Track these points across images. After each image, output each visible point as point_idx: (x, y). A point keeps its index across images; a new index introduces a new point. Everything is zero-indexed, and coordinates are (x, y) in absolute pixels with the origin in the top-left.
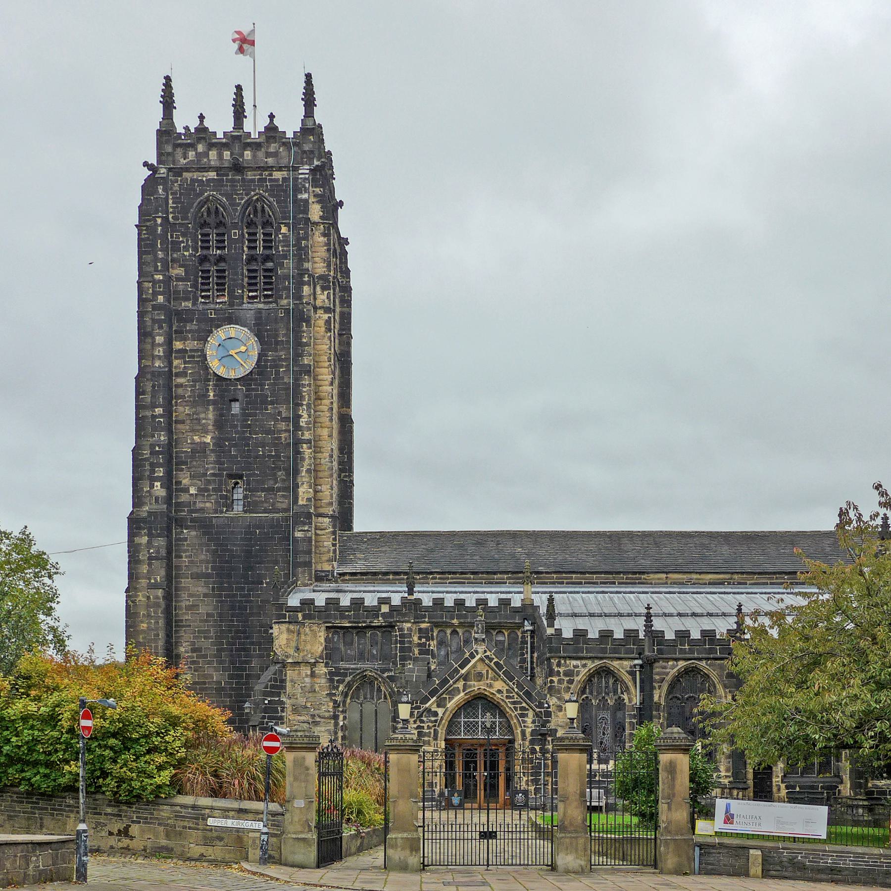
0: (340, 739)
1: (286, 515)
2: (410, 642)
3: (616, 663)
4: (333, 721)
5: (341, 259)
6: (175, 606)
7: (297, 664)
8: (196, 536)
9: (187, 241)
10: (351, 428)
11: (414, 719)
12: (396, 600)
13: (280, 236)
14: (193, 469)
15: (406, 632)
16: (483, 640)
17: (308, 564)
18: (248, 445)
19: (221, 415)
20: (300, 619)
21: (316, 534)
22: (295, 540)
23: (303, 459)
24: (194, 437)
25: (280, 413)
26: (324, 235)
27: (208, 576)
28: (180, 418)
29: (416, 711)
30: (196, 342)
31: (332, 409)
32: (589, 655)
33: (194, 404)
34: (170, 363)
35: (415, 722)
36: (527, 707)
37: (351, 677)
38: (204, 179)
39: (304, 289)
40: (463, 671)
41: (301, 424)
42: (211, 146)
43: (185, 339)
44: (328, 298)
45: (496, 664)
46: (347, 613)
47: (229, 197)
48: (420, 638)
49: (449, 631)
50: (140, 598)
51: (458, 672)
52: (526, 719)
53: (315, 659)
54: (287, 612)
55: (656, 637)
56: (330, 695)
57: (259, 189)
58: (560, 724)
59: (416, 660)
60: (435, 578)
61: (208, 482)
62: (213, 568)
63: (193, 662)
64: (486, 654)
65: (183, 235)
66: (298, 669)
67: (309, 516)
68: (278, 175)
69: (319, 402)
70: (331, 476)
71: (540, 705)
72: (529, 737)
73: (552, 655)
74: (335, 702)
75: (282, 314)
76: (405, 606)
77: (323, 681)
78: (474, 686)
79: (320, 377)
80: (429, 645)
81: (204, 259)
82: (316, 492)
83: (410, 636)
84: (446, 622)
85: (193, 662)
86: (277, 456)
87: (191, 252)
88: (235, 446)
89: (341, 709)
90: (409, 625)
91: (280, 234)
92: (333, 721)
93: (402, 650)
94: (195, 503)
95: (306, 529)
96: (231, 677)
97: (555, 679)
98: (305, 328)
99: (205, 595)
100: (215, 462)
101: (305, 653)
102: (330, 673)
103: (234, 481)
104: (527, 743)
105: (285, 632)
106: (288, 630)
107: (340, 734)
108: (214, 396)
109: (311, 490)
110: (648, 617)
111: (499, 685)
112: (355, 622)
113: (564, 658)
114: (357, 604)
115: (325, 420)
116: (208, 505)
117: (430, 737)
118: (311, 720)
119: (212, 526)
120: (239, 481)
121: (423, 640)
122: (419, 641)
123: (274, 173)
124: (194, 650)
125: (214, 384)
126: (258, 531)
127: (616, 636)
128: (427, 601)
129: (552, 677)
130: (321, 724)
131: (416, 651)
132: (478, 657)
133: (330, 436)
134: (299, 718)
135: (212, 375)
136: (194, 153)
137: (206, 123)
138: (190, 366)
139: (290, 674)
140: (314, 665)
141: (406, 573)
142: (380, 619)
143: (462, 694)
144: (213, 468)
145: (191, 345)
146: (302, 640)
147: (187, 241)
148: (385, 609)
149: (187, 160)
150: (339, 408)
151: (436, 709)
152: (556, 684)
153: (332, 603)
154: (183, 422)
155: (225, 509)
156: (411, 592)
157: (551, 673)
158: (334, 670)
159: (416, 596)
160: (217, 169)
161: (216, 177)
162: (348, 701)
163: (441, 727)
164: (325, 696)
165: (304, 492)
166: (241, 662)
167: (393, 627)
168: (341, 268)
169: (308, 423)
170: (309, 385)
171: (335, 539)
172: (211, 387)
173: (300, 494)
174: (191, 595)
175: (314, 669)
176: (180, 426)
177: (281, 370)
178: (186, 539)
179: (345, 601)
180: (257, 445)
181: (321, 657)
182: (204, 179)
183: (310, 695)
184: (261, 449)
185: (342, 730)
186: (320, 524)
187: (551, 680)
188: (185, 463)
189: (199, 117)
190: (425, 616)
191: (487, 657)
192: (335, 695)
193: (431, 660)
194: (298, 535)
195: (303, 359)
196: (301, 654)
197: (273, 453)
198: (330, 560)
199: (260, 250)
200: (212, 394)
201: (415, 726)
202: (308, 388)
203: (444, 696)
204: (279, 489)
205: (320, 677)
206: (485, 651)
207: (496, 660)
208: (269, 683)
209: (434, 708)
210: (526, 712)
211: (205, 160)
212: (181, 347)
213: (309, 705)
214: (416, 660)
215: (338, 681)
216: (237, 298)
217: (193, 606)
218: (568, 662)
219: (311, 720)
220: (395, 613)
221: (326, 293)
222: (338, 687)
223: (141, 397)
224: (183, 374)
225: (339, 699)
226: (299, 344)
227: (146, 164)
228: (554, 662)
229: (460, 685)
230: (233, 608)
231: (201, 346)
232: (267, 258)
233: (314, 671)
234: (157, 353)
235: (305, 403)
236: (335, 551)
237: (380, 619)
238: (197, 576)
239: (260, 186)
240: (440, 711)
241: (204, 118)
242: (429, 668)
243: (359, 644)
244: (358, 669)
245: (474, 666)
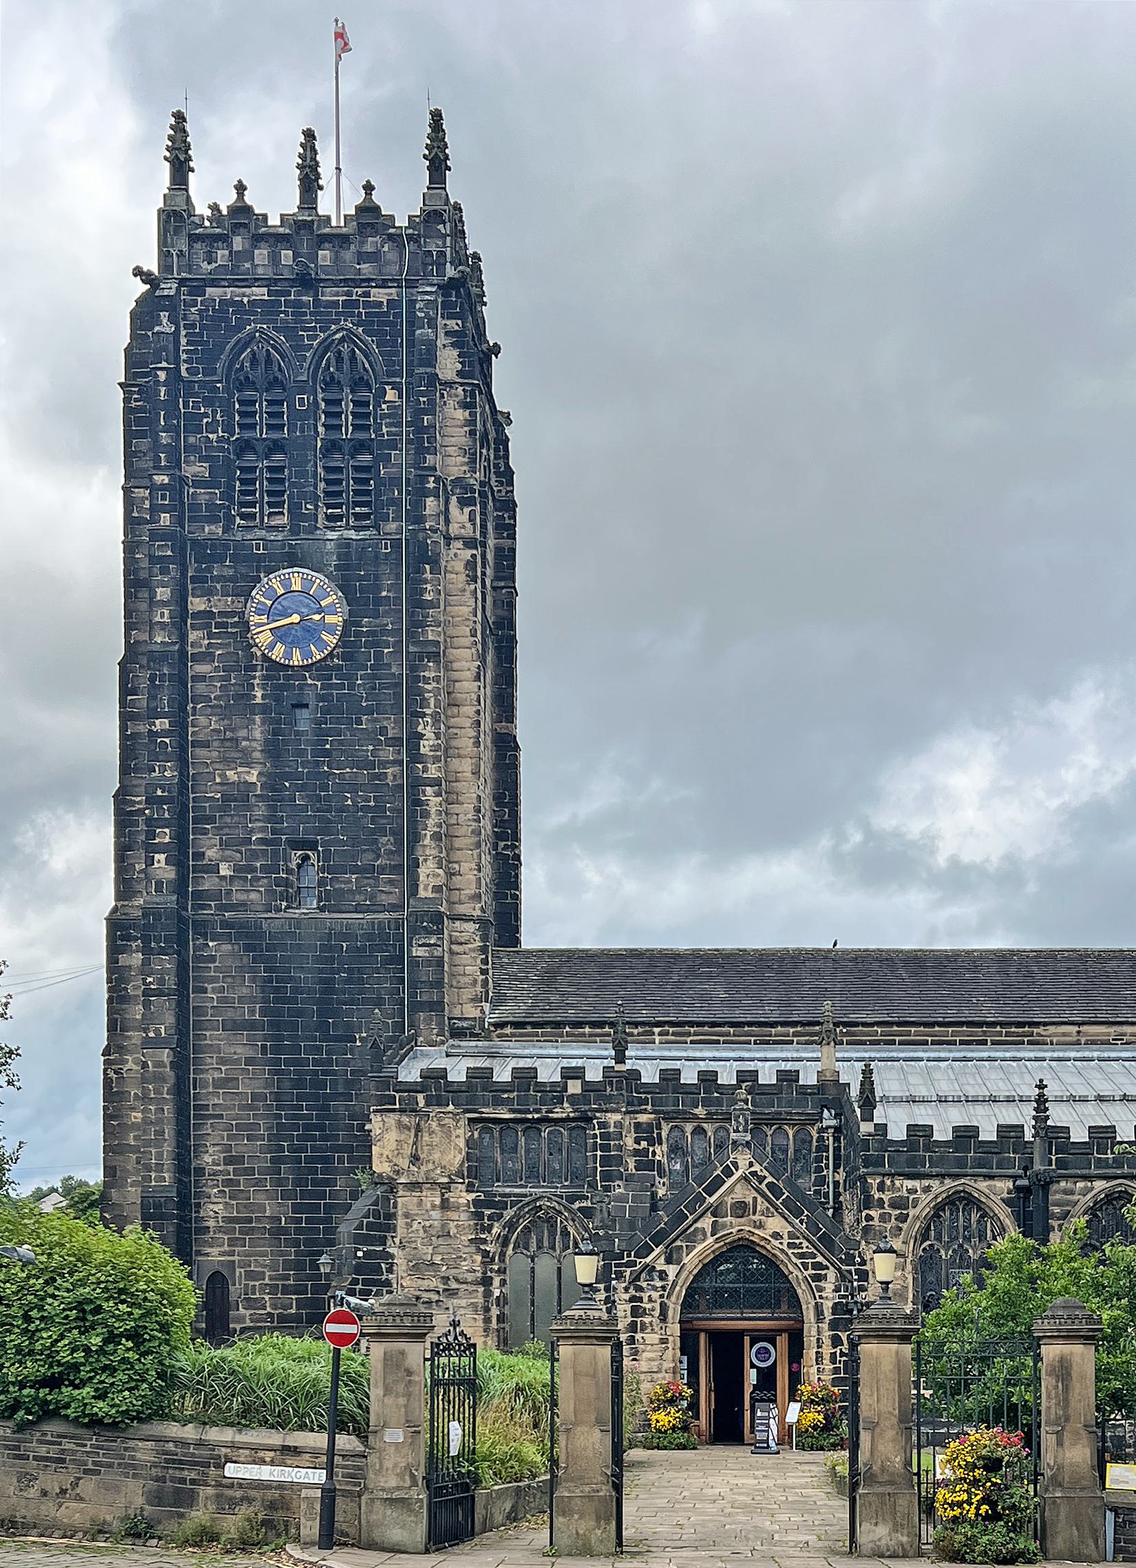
0: (494, 1320)
1: (395, 915)
2: (620, 1148)
3: (983, 1185)
4: (481, 1289)
5: (497, 450)
6: (195, 1079)
7: (414, 1186)
8: (232, 954)
9: (214, 412)
10: (516, 758)
11: (624, 1285)
12: (594, 1074)
13: (384, 406)
14: (226, 831)
15: (612, 1130)
16: (748, 1144)
17: (437, 1006)
18: (325, 787)
19: (276, 733)
21: (452, 952)
22: (414, 962)
23: (426, 815)
24: (228, 773)
25: (383, 730)
26: (465, 406)
27: (251, 1026)
28: (201, 737)
29: (629, 1270)
30: (230, 599)
31: (479, 723)
32: (935, 1170)
33: (225, 712)
34: (183, 637)
35: (626, 1290)
36: (825, 1263)
37: (515, 1209)
38: (245, 300)
39: (428, 503)
40: (711, 1200)
41: (422, 751)
42: (257, 239)
43: (210, 593)
44: (472, 519)
45: (769, 1185)
46: (506, 1096)
47: (290, 332)
48: (637, 1141)
49: (689, 1128)
50: (130, 1065)
51: (700, 1199)
52: (822, 1284)
53: (449, 1177)
55: (1054, 1137)
56: (477, 1242)
57: (345, 320)
59: (629, 1179)
60: (667, 1034)
61: (254, 855)
62: (264, 1012)
63: (228, 1183)
64: (752, 1169)
65: (208, 402)
67: (438, 918)
68: (380, 295)
69: (455, 710)
70: (478, 845)
71: (850, 1260)
72: (828, 1315)
74: (485, 1254)
75: (386, 549)
76: (611, 1083)
77: (461, 1219)
78: (732, 1226)
79: (455, 666)
80: (654, 1153)
81: (245, 446)
82: (450, 874)
83: (620, 1136)
84: (685, 1112)
85: (228, 1183)
86: (380, 809)
87: (221, 434)
88: (302, 788)
89: (496, 1268)
90: (617, 1117)
91: (385, 402)
92: (481, 1289)
93: (605, 1161)
94: (229, 892)
95: (432, 942)
96: (297, 1208)
98: (428, 576)
99: (249, 1061)
100: (268, 819)
101: (431, 1166)
102: (476, 1202)
103: (300, 852)
104: (825, 1326)
105: (394, 1128)
106: (401, 1126)
107: (495, 1311)
108: (263, 697)
109: (441, 871)
110: (1041, 1102)
111: (775, 1224)
112: (519, 1111)
113: (892, 1175)
114: (525, 1078)
115: (465, 743)
116: (253, 896)
118: (441, 1287)
119: (260, 935)
120: (309, 853)
121: (644, 1144)
122: (636, 1146)
123: (373, 291)
124: (229, 1161)
125: (263, 675)
126: (344, 944)
127: (937, 1136)
128: (650, 1076)
130: (460, 1294)
131: (631, 1165)
132: (737, 1175)
133: (476, 773)
134: (420, 1281)
135: (260, 659)
136: (227, 252)
137: (249, 199)
138: (219, 641)
139: (405, 1201)
140: (447, 1187)
141: (612, 1024)
142: (566, 1105)
143: (711, 1240)
144: (263, 829)
145: (220, 603)
146: (424, 1144)
147: (214, 412)
148: (574, 1087)
149: (214, 265)
150: (493, 722)
151: (664, 1268)
152: (876, 1222)
153: (481, 1077)
154: (206, 745)
155: (284, 904)
156: (620, 1059)
157: (867, 1202)
158: (482, 1198)
159: (629, 1065)
160: (268, 283)
161: (266, 298)
162: (510, 1251)
163: (673, 1298)
164: (467, 1243)
165: (430, 876)
166: (315, 1182)
168: (496, 466)
169: (435, 748)
170: (437, 679)
171: (485, 962)
172: (257, 681)
173: (421, 879)
174: (222, 1061)
175: (446, 1196)
176: (201, 752)
177: (386, 651)
178: (212, 959)
179: (503, 1074)
180: (341, 788)
181: (460, 1174)
182: (245, 300)
183: (441, 1241)
184: (349, 795)
185: (498, 1305)
186: (458, 934)
188: (211, 820)
189: (236, 187)
191: (754, 1174)
192: (484, 1241)
193: (657, 1179)
194: (419, 952)
195: (424, 633)
196: (424, 1168)
197: (372, 804)
198: (476, 1000)
199: (347, 433)
200: (259, 694)
201: (627, 1296)
202: (434, 684)
203: (678, 1243)
204: (382, 869)
205: (457, 1208)
206: (751, 1165)
207: (770, 1179)
208: (365, 1220)
209: (661, 1265)
210: (823, 1272)
211: (247, 265)
212: (202, 608)
213: (437, 1259)
214: (629, 1179)
215: (490, 1218)
216: (304, 518)
217: (227, 1080)
218: (897, 1183)
219: (441, 1287)
221: (467, 510)
222: (490, 1228)
223: (129, 698)
224: (207, 657)
225: (490, 1248)
226: (417, 603)
227: (138, 272)
228: (874, 1182)
229: (706, 1223)
230: (299, 1083)
231: (240, 605)
232: (360, 447)
233: (448, 1199)
234: (158, 619)
235: (428, 711)
236: (485, 983)
237: (566, 1105)
238: (233, 1026)
239: (347, 315)
240: (672, 1270)
241: (245, 189)
242: (654, 1195)
243: (528, 1151)
245: (731, 1190)
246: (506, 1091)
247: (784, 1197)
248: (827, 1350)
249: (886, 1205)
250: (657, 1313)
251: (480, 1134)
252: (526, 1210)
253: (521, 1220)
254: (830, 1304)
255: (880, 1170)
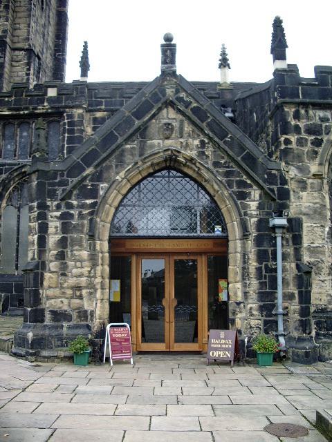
11: (56, 203)
15: (76, 119)
35: (58, 207)
36: (249, 182)
37: (7, 174)
45: (195, 110)
46: (6, 99)
58: (304, 210)
72: (253, 232)
73: (287, 100)
83: (81, 123)
90: (80, 111)
93: (70, 140)
97: (293, 138)
104: (250, 244)
113: (305, 105)
117: (82, 232)
129: (286, 134)
142: (46, 104)
152: (294, 146)
157: (286, 129)
167: (60, 114)
187: (286, 139)
190: (100, 104)
191: (180, 100)
201: (58, 214)
218: (311, 112)
220: (64, 97)
228: (290, 111)
243: (21, 137)
244: (15, 165)
246: (7, 97)
247: (209, 120)
248: (253, 265)
249: (302, 130)
250: (86, 229)
252: (15, 174)
253: (12, 183)
254: (254, 220)
255: (297, 100)
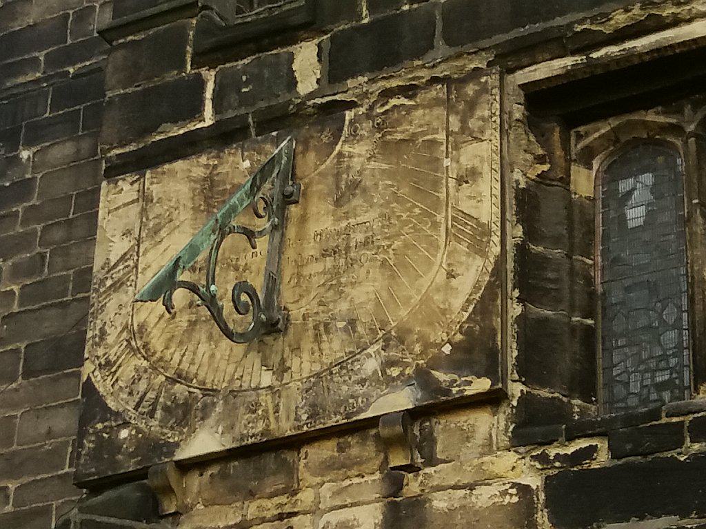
20: (306, 85)
53: (423, 378)
54: (204, 57)
66: (270, 506)
101: (335, 347)
158: (603, 458)
175: (413, 487)
196: (303, 366)
251: (611, 175)
